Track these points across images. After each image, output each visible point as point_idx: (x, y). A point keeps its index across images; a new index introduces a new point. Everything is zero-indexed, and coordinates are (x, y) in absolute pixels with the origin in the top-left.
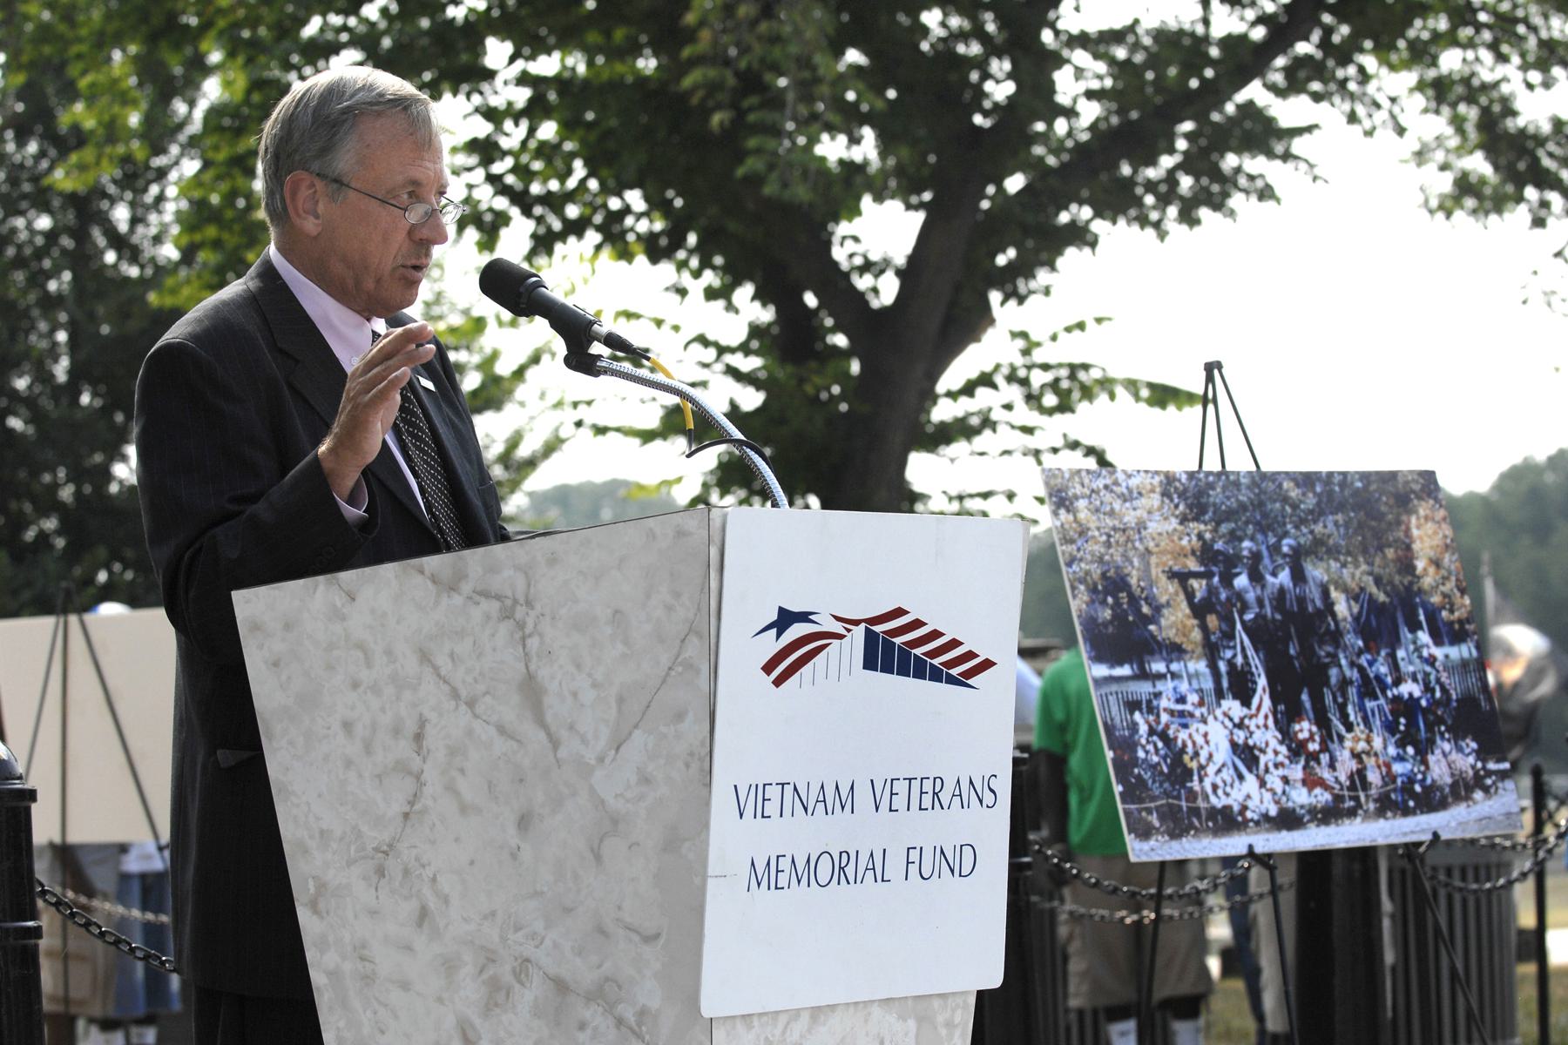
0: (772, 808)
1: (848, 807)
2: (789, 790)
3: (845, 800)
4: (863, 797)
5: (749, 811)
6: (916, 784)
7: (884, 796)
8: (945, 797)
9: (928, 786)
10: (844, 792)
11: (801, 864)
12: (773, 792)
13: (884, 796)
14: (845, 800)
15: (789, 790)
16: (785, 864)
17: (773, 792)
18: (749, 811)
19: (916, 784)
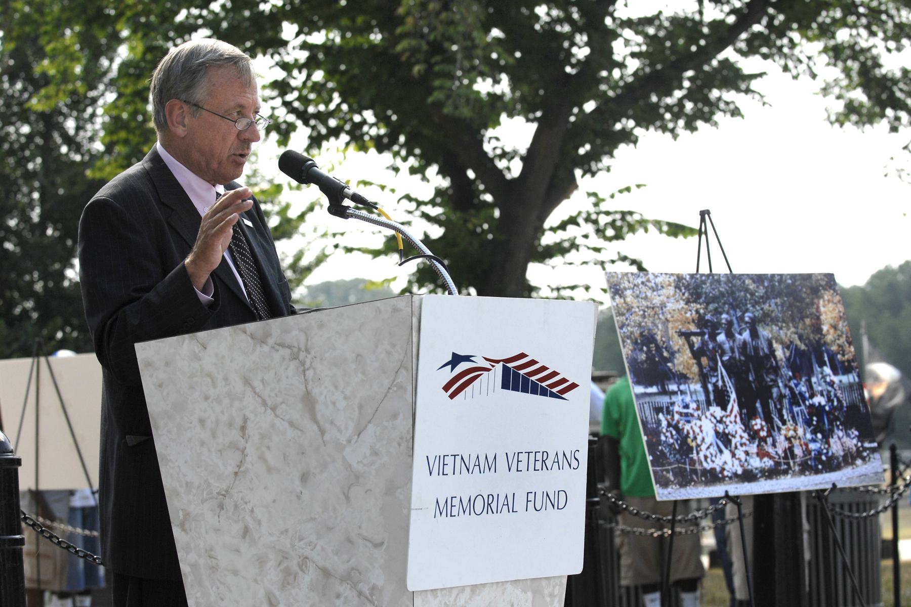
0: (448, 469)
1: (493, 469)
2: (458, 459)
3: (491, 464)
4: (502, 463)
5: (435, 471)
6: (532, 456)
7: (514, 462)
8: (549, 463)
9: (539, 456)
10: (491, 460)
11: (465, 502)
12: (449, 460)
13: (514, 462)
14: (491, 464)
15: (458, 459)
16: (456, 502)
17: (449, 460)
18: (435, 471)
19: (532, 456)
